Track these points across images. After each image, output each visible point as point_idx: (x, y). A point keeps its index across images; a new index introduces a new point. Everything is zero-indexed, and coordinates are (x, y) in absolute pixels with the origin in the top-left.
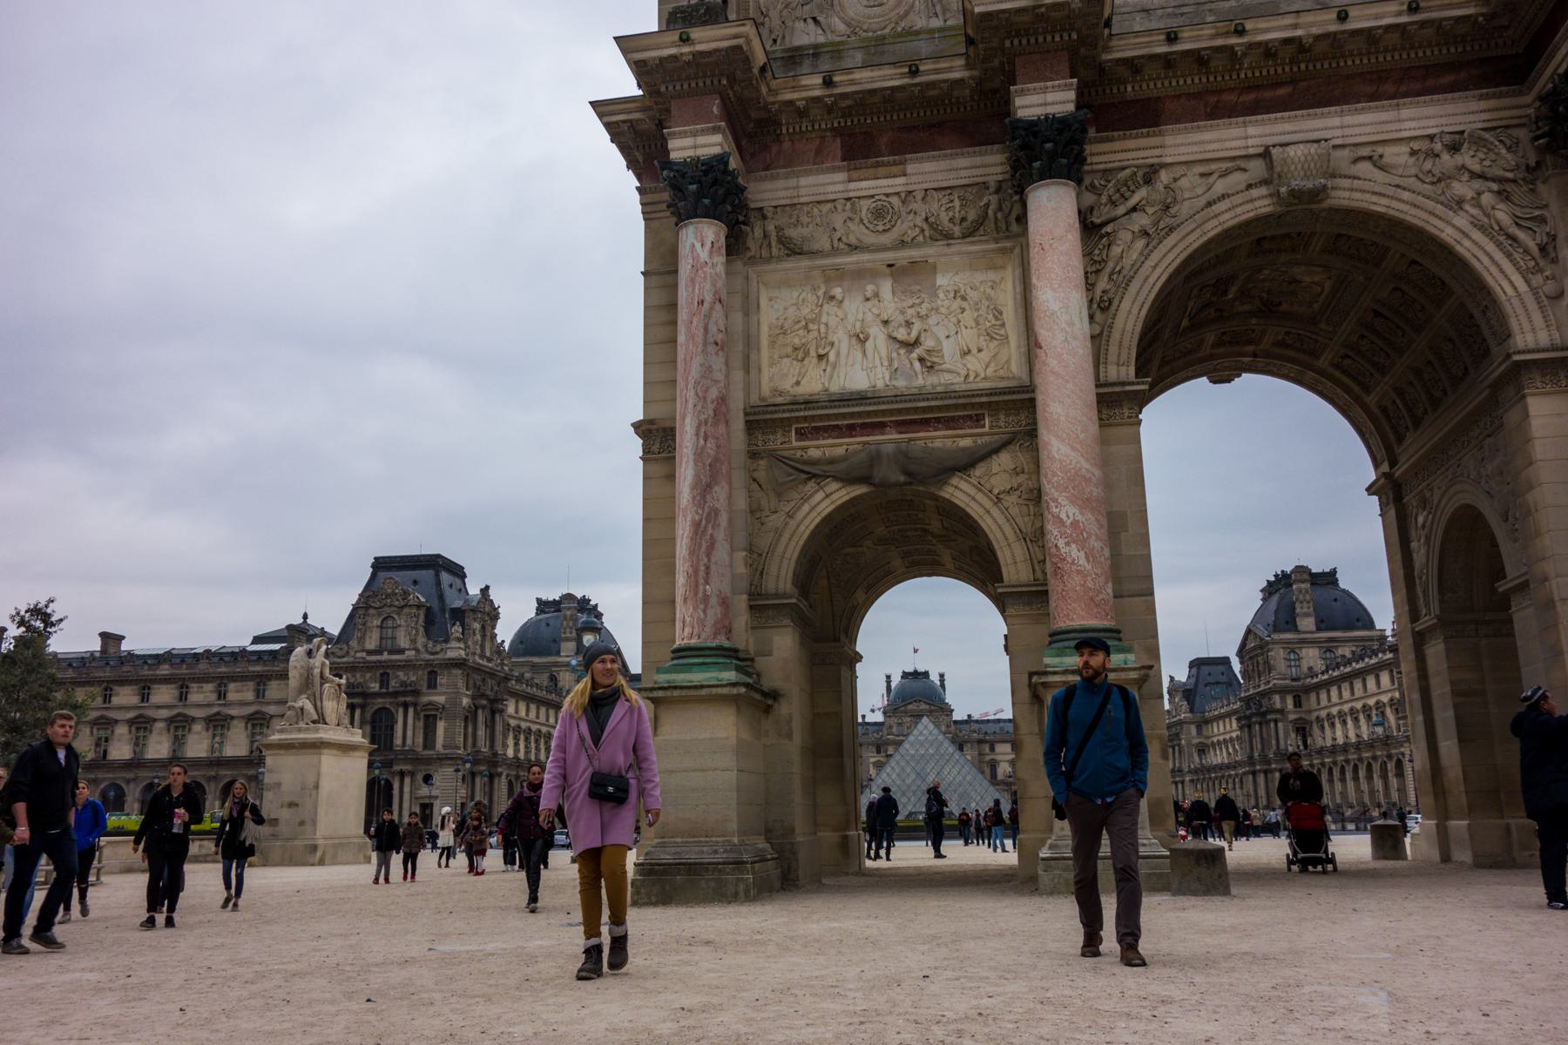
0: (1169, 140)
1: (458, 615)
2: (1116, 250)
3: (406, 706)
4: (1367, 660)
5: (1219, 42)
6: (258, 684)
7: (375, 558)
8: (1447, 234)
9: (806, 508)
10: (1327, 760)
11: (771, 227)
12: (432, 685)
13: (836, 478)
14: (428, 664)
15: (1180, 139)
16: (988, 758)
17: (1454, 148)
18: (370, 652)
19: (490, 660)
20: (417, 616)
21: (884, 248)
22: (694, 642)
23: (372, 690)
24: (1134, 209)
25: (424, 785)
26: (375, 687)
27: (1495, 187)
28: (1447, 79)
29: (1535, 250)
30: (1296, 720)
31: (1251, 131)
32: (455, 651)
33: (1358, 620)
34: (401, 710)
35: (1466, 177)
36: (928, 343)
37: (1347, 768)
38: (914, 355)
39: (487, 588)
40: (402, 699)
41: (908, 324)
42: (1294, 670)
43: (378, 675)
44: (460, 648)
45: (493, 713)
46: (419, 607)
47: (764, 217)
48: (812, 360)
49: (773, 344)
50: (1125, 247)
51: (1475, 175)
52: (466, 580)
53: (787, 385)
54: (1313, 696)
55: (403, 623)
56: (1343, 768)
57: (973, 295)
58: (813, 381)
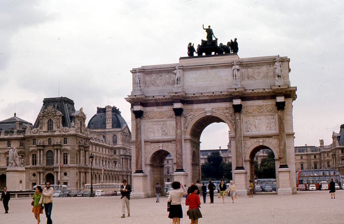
0: (194, 106)
1: (72, 118)
3: (57, 150)
5: (199, 95)
6: (8, 142)
7: (44, 99)
12: (65, 142)
14: (64, 135)
15: (196, 106)
17: (226, 109)
18: (44, 132)
20: (60, 119)
23: (46, 145)
24: (190, 115)
25: (65, 176)
26: (47, 143)
27: (230, 114)
29: (233, 123)
32: (72, 132)
34: (56, 151)
35: (227, 113)
36: (166, 131)
38: (164, 133)
39: (82, 108)
40: (55, 147)
41: (164, 128)
43: (48, 139)
44: (74, 130)
45: (85, 151)
46: (60, 116)
47: (146, 113)
51: (229, 113)
52: (74, 105)
55: (55, 121)
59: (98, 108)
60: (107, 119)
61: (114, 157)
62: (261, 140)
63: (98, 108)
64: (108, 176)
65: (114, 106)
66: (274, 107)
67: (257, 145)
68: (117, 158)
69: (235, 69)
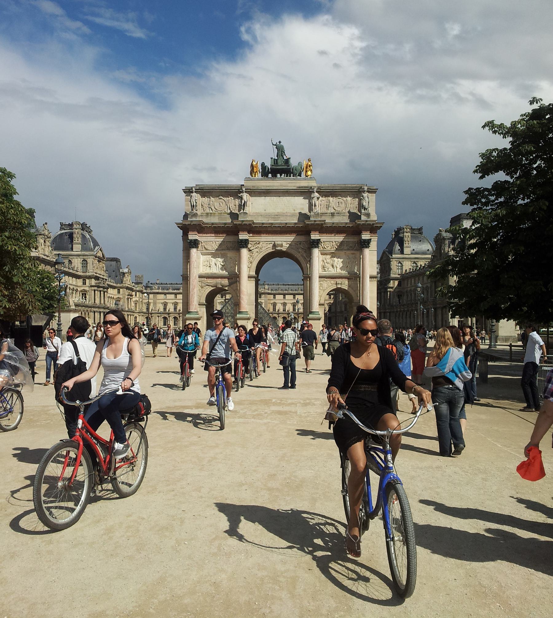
0: (262, 238)
2: (253, 254)
4: (425, 269)
8: (298, 257)
9: (207, 290)
10: (406, 309)
11: (203, 245)
13: (211, 286)
16: (272, 302)
17: (300, 244)
19: (48, 256)
21: (220, 250)
22: (191, 311)
28: (301, 233)
30: (398, 291)
31: (274, 238)
33: (428, 250)
37: (412, 313)
42: (399, 270)
47: (202, 243)
48: (208, 267)
49: (202, 263)
50: (255, 254)
53: (204, 270)
54: (406, 282)
56: (411, 312)
57: (233, 258)
58: (208, 271)
59: (62, 224)
60: (74, 239)
61: (82, 288)
62: (339, 281)
63: (62, 224)
64: (84, 313)
65: (84, 223)
66: (356, 245)
67: (334, 287)
68: (87, 289)
69: (315, 197)
